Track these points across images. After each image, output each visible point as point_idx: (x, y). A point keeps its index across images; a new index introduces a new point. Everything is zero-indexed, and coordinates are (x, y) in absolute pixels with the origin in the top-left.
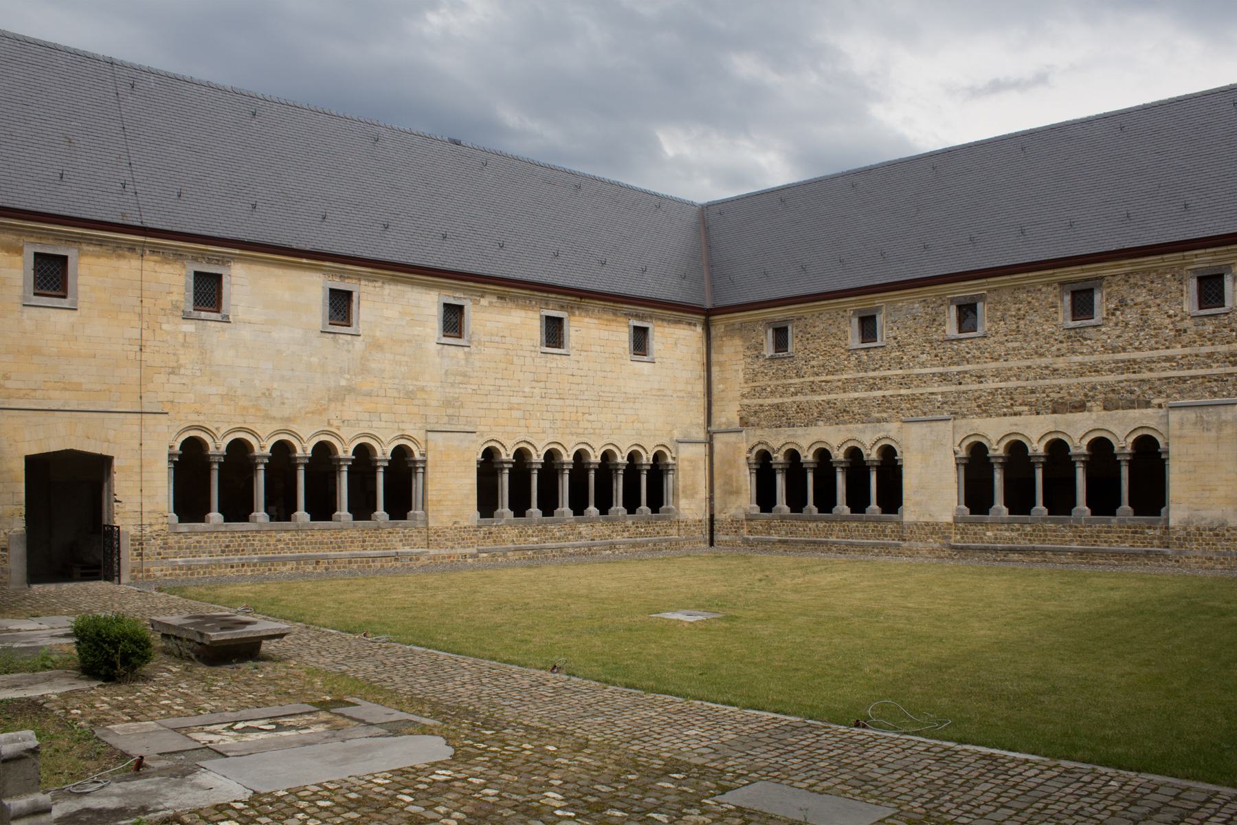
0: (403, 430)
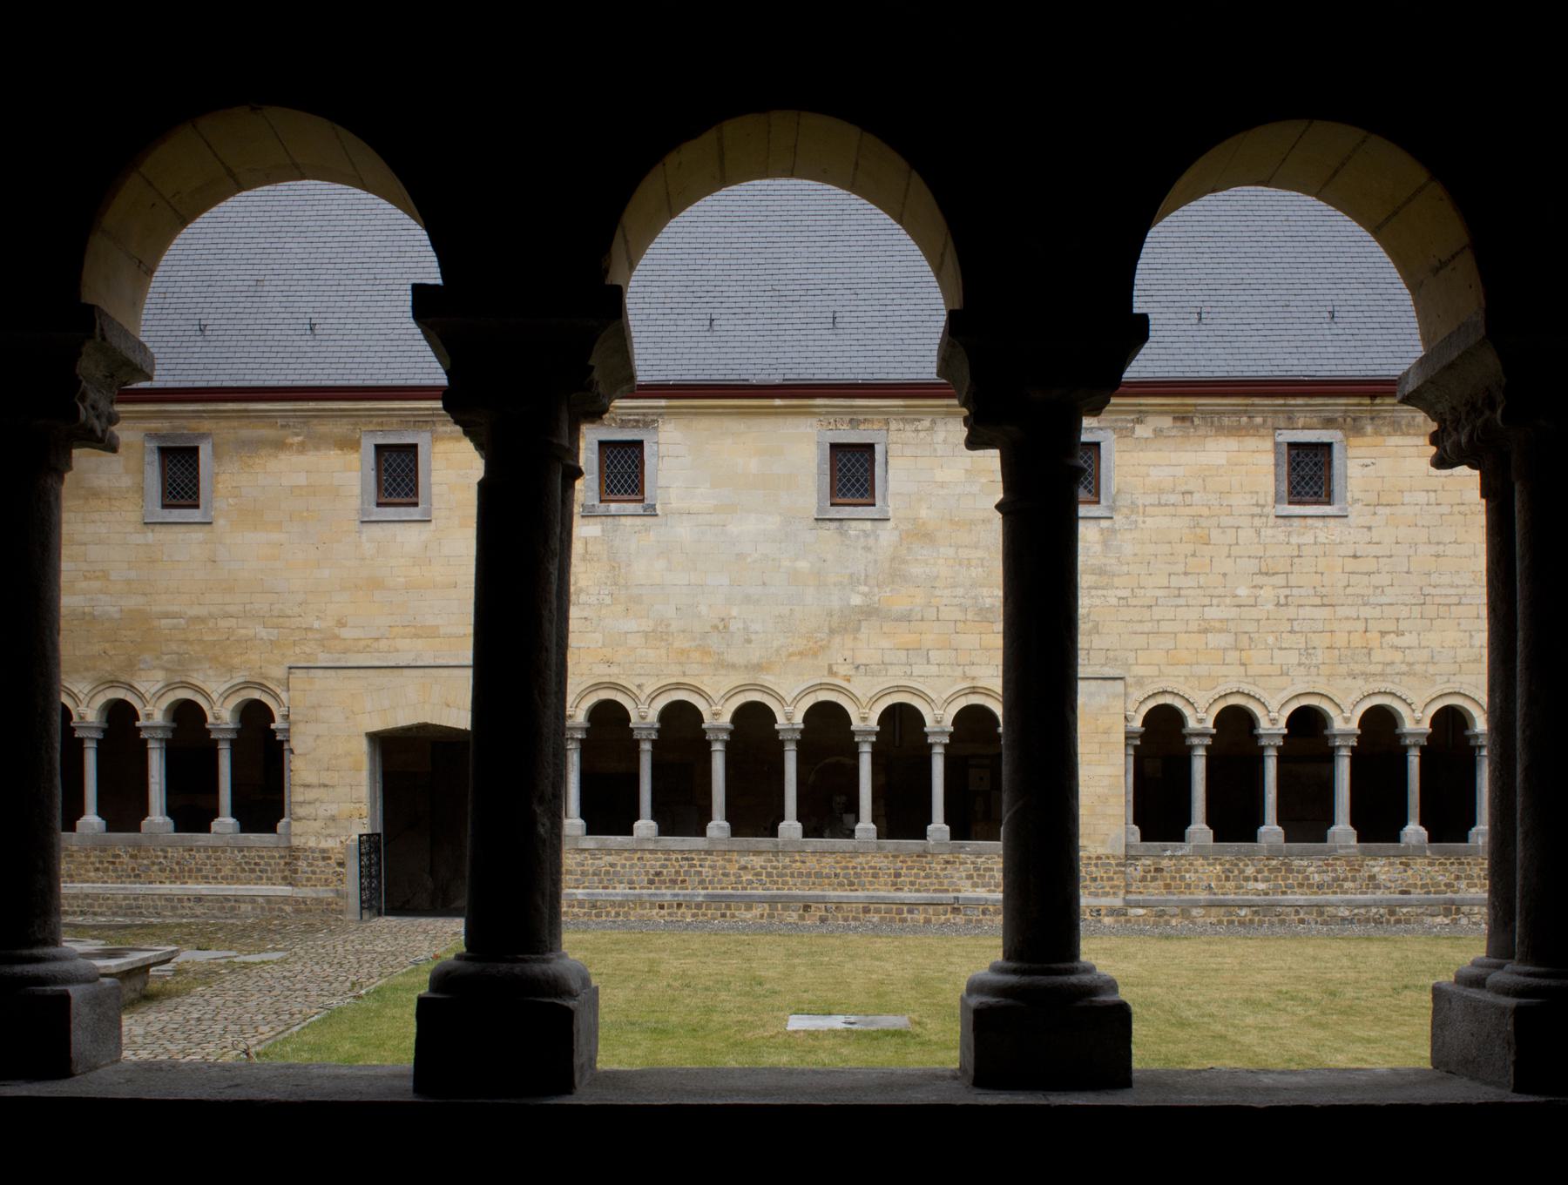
0: (974, 678)
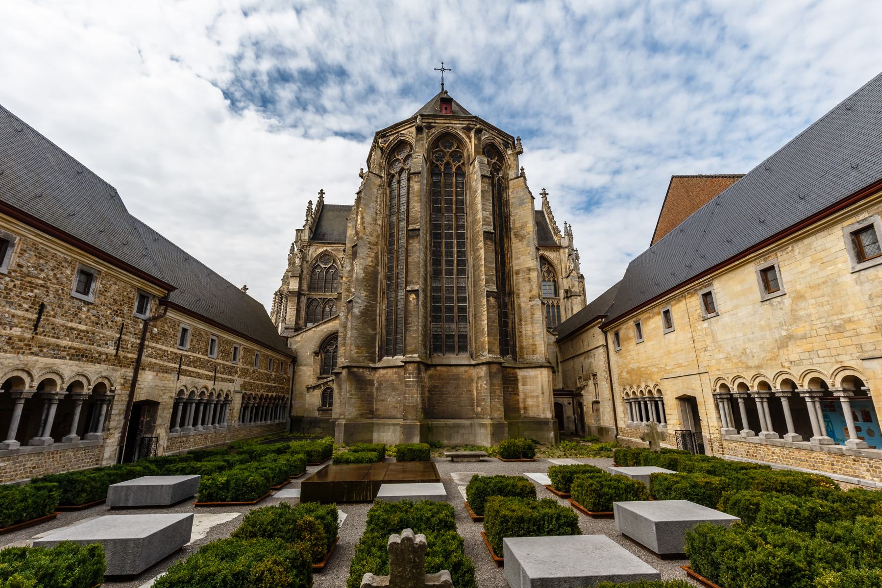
0: (841, 362)
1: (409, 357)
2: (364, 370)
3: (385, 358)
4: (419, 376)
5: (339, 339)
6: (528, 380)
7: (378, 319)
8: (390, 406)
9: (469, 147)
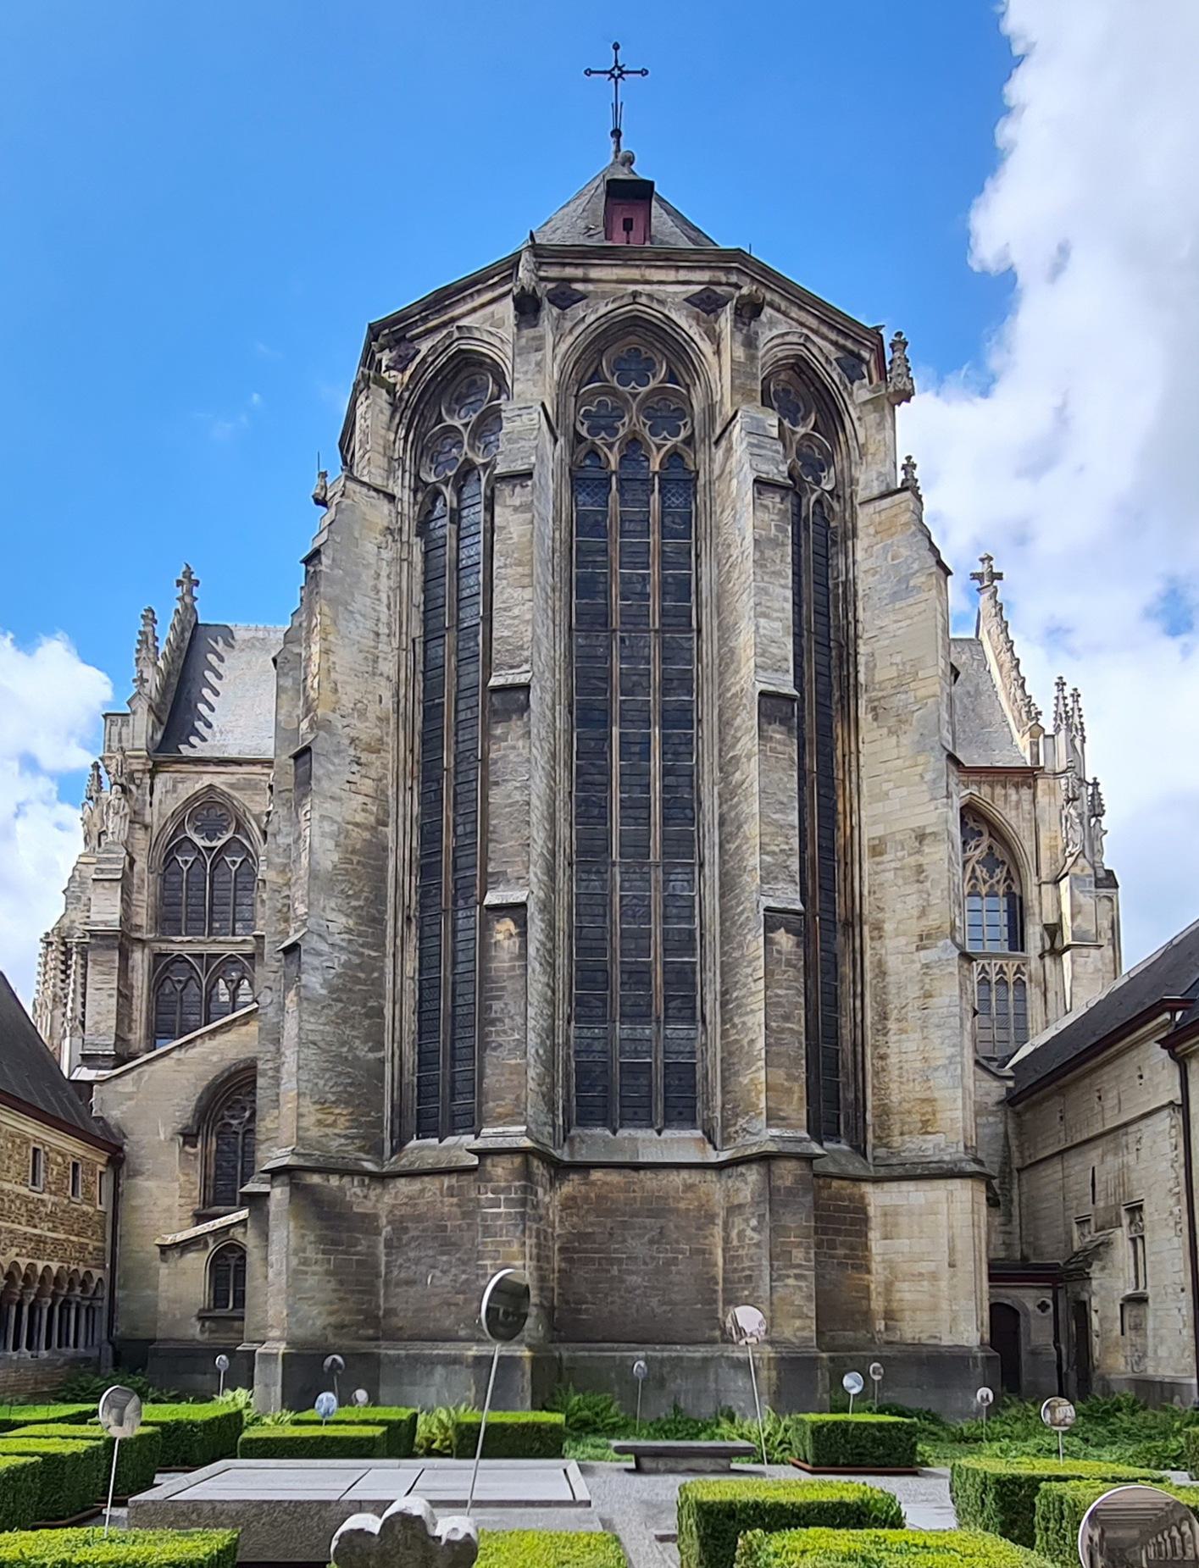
1: (492, 1135)
2: (346, 1180)
3: (414, 1143)
4: (526, 1199)
5: (261, 1082)
6: (903, 1220)
7: (388, 1012)
8: (435, 1301)
9: (713, 374)
